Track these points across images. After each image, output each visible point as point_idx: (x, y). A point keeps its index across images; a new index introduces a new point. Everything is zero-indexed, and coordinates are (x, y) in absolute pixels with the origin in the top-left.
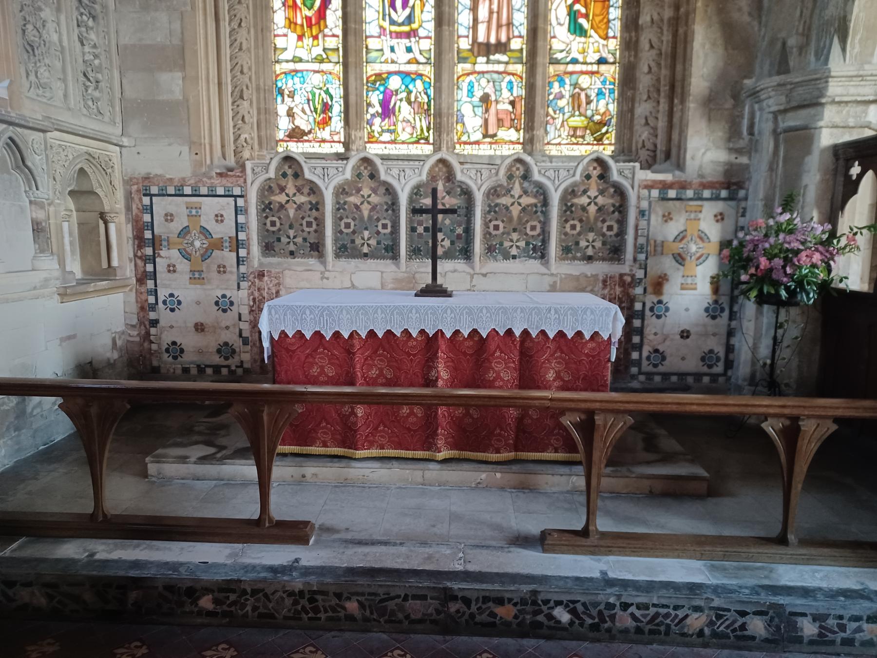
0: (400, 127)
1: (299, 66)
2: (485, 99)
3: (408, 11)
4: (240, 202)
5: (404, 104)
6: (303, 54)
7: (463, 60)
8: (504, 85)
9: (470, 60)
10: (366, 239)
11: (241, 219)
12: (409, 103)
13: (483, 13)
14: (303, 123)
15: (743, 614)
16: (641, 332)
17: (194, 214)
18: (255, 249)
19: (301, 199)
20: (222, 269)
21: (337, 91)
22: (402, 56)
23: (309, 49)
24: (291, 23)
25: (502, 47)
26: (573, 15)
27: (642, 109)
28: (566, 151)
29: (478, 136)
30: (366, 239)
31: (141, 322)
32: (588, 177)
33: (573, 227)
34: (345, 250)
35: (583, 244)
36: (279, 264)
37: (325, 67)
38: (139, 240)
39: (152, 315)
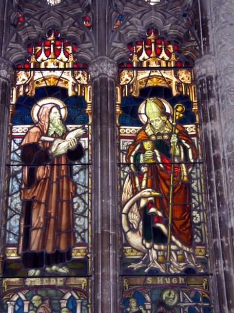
8: (64, 304)
9: (19, 274)
13: (37, 218)
25: (61, 257)
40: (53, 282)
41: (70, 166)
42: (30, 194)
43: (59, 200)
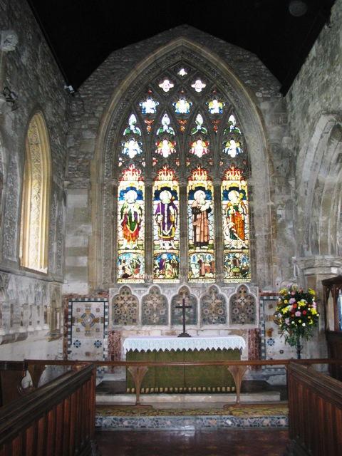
0: (166, 273)
1: (127, 251)
2: (200, 262)
3: (169, 231)
4: (106, 304)
5: (168, 265)
6: (129, 247)
7: (191, 248)
10: (155, 317)
11: (106, 310)
12: (170, 262)
13: (198, 231)
14: (128, 272)
15: (279, 418)
16: (265, 351)
17: (88, 310)
18: (111, 322)
19: (130, 302)
20: (98, 330)
21: (142, 260)
22: (167, 247)
23: (131, 245)
24: (125, 236)
25: (206, 244)
26: (231, 232)
27: (259, 266)
28: (232, 281)
29: (198, 276)
30: (155, 317)
31: (64, 352)
32: (240, 292)
33: (236, 311)
34: (147, 321)
35: (240, 317)
36: (121, 328)
37: (138, 251)
38: (66, 319)
39: (69, 349)
40: (203, 251)
41: (207, 214)
43: (204, 226)
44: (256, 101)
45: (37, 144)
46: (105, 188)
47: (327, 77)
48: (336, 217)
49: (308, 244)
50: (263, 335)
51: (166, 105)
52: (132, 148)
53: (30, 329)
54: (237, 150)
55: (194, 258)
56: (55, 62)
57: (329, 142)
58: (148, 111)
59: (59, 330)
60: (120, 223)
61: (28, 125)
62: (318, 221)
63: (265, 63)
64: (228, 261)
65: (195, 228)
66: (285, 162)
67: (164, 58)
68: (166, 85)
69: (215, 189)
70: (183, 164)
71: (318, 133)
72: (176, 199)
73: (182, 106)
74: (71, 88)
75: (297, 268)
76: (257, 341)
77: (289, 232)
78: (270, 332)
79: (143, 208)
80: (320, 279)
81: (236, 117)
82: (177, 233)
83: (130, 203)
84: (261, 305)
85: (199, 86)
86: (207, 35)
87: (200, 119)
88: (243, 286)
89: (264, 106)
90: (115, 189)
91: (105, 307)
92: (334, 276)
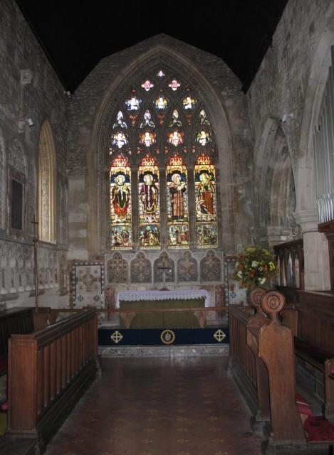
2: (177, 232)
4: (103, 267)
6: (119, 220)
7: (170, 221)
11: (103, 272)
12: (152, 233)
13: (175, 208)
14: (120, 241)
17: (88, 271)
18: (107, 281)
19: (121, 265)
20: (96, 288)
21: (130, 231)
22: (150, 220)
24: (116, 212)
25: (183, 217)
38: (71, 280)
39: (74, 303)
42: (172, 201)
44: (221, 98)
45: (45, 143)
46: (99, 173)
47: (271, 88)
48: (286, 195)
49: (262, 217)
50: (226, 290)
51: (148, 104)
52: (120, 140)
53: (46, 286)
54: (207, 139)
55: (172, 229)
56: (57, 76)
57: (276, 138)
58: (133, 108)
59: (66, 288)
60: (112, 202)
61: (39, 134)
62: (270, 198)
63: (229, 65)
64: (200, 231)
65: (172, 204)
66: (244, 149)
67: (146, 62)
68: (147, 86)
69: (188, 172)
70: (162, 153)
71: (266, 130)
72: (157, 181)
73: (161, 103)
74: (69, 93)
75: (254, 236)
76: (222, 294)
77: (248, 207)
78: (232, 288)
79: (130, 188)
80: (271, 245)
81: (205, 111)
82: (158, 209)
83: (121, 185)
84: (225, 266)
85: (175, 85)
86: (181, 42)
87: (176, 114)
88: (211, 251)
89: (229, 103)
90: (108, 174)
91: (101, 269)
92: (282, 243)
